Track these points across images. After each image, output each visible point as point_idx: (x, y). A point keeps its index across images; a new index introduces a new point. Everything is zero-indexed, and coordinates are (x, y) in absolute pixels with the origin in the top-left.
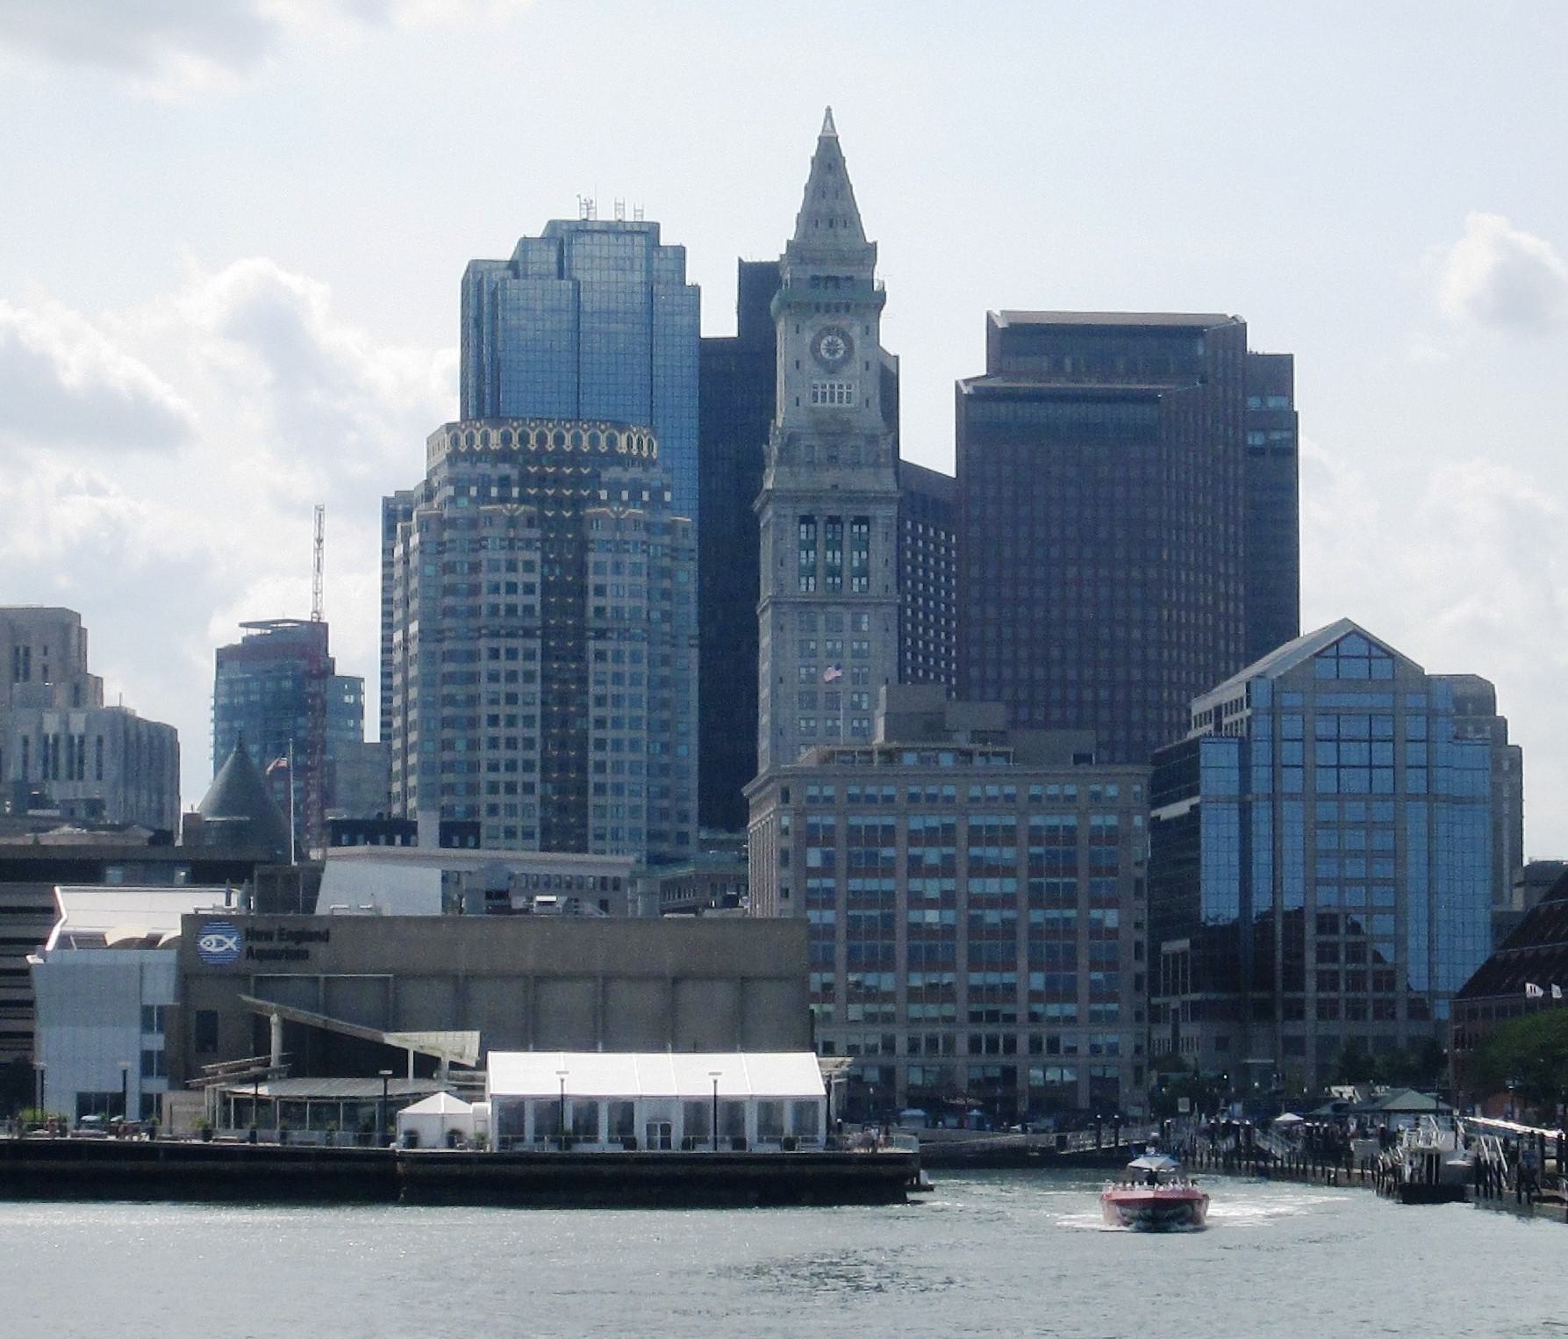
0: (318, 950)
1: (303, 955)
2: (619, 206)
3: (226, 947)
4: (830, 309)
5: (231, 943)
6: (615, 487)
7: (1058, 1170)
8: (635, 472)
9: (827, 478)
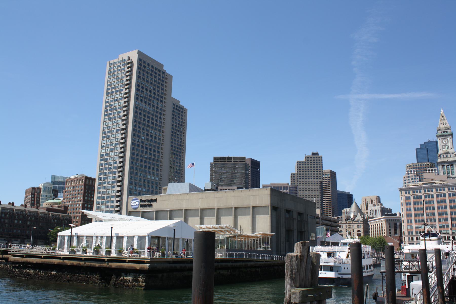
0: (154, 204)
1: (151, 206)
2: (433, 139)
3: (136, 204)
4: (444, 136)
5: (137, 203)
6: (429, 170)
7: (56, 263)
8: (432, 168)
9: (445, 160)
